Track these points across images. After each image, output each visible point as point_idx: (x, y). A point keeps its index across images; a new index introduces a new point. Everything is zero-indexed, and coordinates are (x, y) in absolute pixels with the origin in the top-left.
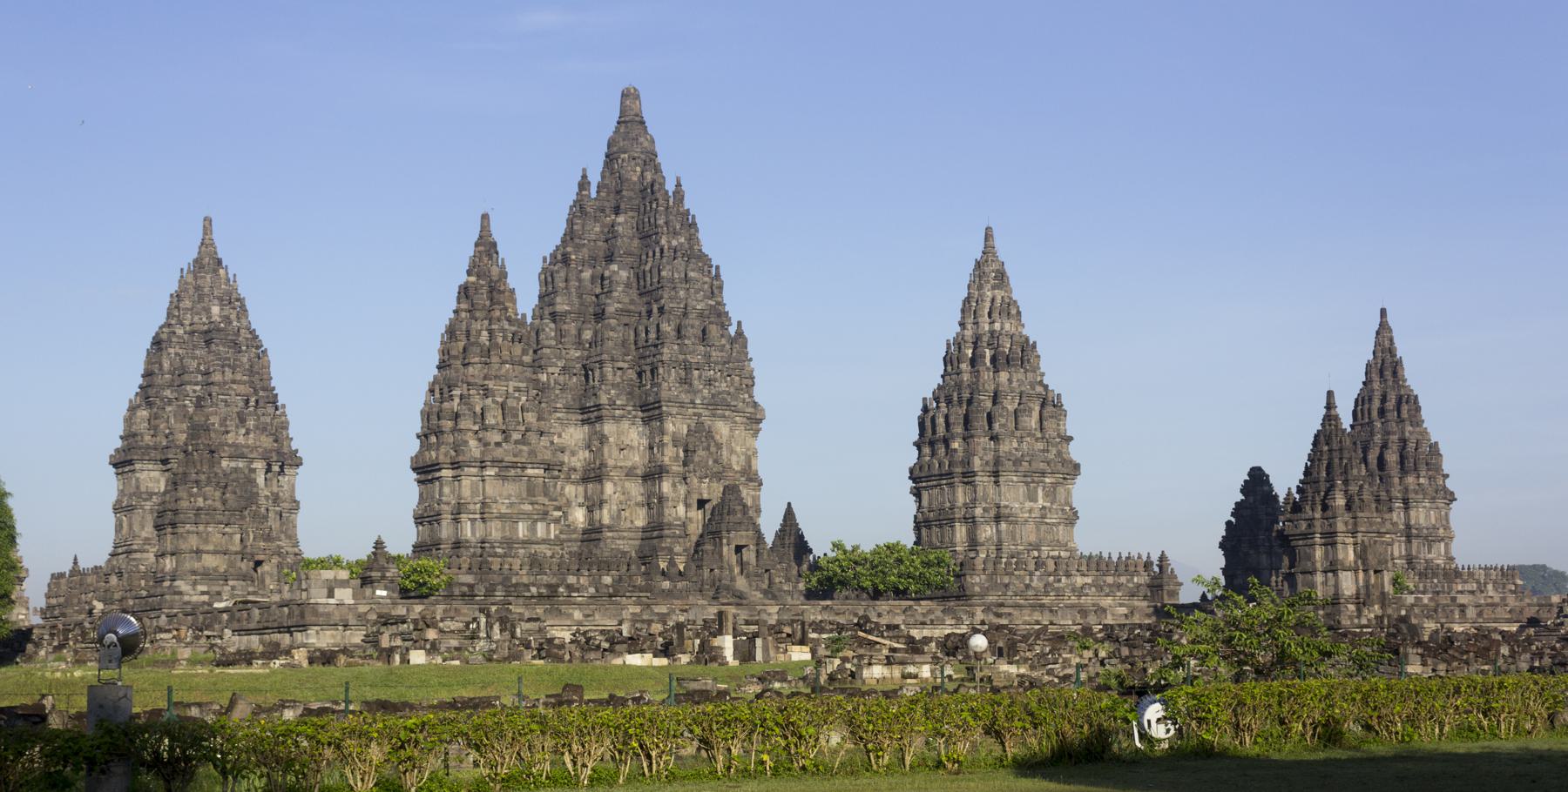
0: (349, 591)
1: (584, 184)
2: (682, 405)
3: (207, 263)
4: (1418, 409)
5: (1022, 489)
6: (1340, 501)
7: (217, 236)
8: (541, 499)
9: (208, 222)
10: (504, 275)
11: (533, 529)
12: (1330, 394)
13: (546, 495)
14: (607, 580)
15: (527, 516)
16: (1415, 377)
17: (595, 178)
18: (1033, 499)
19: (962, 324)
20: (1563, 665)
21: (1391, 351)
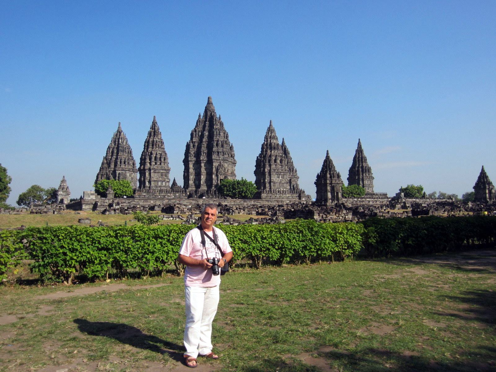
0: (94, 196)
1: (200, 116)
2: (217, 160)
3: (119, 132)
4: (366, 160)
5: (276, 176)
6: (328, 176)
7: (121, 126)
8: (164, 177)
9: (119, 123)
10: (158, 129)
11: (162, 184)
12: (327, 151)
13: (165, 176)
14: (177, 195)
15: (161, 181)
16: (366, 153)
17: (202, 115)
18: (279, 178)
19: (265, 140)
20: (52, 258)
21: (361, 148)
